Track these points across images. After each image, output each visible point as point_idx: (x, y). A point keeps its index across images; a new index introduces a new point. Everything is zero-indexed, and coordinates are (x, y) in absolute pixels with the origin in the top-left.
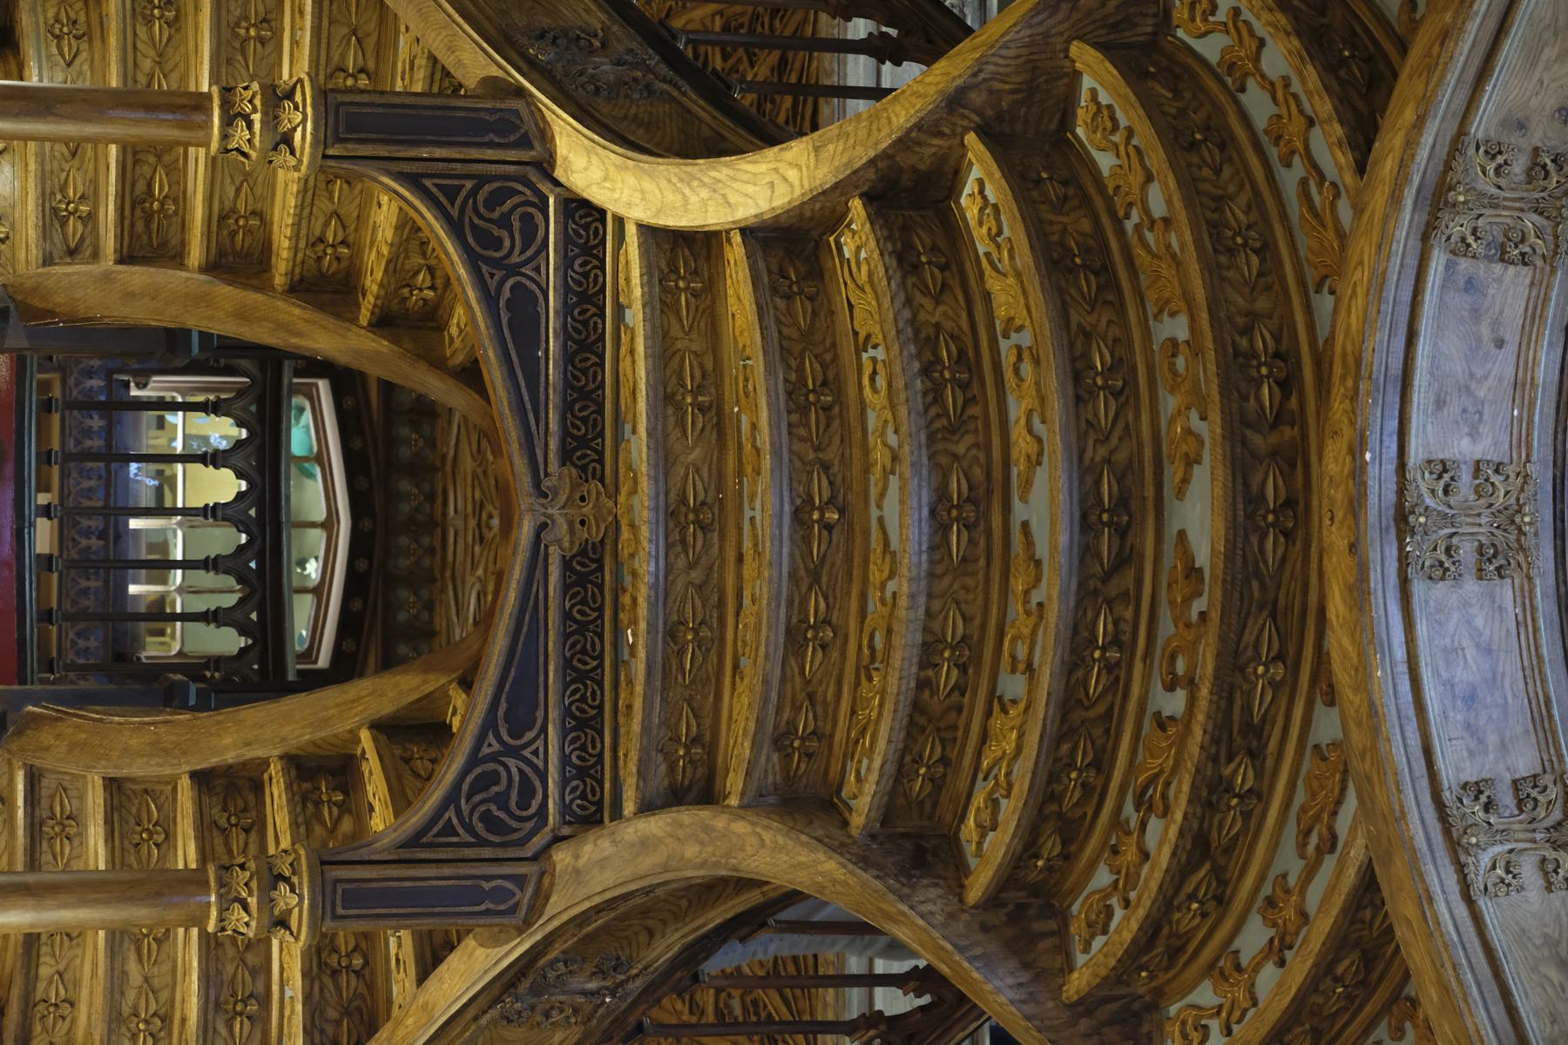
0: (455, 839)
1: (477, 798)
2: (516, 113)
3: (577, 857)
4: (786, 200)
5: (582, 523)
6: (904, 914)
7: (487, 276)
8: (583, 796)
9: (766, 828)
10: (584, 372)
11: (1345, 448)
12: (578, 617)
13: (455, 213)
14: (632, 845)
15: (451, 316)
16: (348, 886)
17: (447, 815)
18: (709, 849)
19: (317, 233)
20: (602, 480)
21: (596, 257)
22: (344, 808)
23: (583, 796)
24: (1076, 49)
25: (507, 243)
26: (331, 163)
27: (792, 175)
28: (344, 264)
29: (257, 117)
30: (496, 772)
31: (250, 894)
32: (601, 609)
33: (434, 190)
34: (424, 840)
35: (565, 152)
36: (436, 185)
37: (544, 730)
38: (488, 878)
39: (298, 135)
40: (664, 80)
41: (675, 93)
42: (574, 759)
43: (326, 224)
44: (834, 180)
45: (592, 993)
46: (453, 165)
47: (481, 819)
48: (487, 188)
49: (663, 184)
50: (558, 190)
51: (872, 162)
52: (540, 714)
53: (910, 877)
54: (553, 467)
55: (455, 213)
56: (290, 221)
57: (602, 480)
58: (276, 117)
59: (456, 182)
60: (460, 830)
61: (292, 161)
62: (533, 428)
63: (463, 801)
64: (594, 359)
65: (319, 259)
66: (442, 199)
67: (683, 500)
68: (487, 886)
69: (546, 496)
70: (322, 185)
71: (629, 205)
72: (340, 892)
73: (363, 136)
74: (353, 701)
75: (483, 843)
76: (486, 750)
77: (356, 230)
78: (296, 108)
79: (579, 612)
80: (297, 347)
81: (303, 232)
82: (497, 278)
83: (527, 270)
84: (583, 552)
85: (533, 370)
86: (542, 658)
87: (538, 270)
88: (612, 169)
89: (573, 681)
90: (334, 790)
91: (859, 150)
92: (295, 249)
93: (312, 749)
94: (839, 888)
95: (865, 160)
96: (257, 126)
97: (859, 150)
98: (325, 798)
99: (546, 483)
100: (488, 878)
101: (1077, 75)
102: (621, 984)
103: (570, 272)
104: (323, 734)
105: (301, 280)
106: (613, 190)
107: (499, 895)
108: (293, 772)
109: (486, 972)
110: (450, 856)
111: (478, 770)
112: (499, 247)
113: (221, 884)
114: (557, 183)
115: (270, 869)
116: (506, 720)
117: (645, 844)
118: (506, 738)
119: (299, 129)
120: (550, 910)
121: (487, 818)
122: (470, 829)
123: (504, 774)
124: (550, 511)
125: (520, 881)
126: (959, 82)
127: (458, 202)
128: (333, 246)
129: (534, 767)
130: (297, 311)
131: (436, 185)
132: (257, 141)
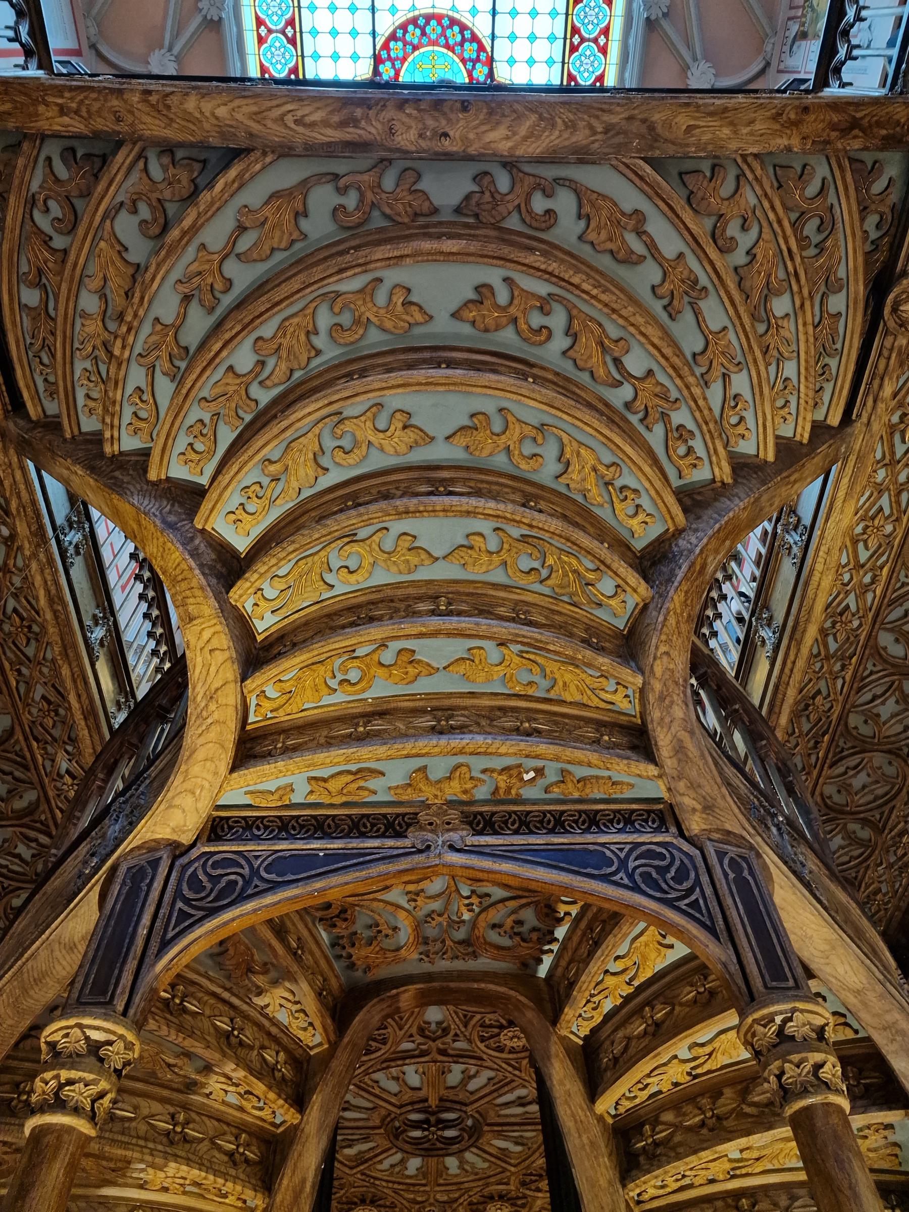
0: (701, 902)
2: (129, 869)
3: (694, 810)
4: (223, 636)
5: (448, 823)
6: (702, 551)
8: (646, 821)
9: (657, 648)
10: (337, 826)
11: (401, 116)
12: (516, 826)
13: (201, 914)
14: (679, 761)
15: (297, 1042)
16: (767, 977)
18: (675, 698)
19: (226, 1158)
20: (417, 814)
21: (254, 822)
22: (655, 1122)
23: (646, 821)
24: (152, 475)
25: (233, 877)
26: (131, 1012)
27: (206, 635)
28: (254, 1141)
29: (65, 1074)
30: (641, 875)
31: (804, 1060)
32: (510, 814)
33: (177, 930)
34: (708, 923)
35: (168, 830)
37: (603, 845)
39: (95, 1035)
40: (137, 790)
41: (148, 781)
42: (621, 826)
43: (220, 1148)
44: (213, 599)
45: (779, 829)
46: (161, 915)
47: (681, 883)
48: (186, 892)
49: (201, 741)
50: (198, 845)
51: (203, 574)
52: (591, 847)
53: (674, 556)
55: (201, 914)
56: (211, 1177)
57: (417, 814)
58: (70, 1056)
59: (175, 914)
60: (693, 898)
61: (119, 1046)
64: (329, 821)
65: (247, 1161)
67: (433, 728)
68: (732, 876)
69: (429, 847)
70: (187, 1146)
71: (216, 773)
72: (774, 983)
73: (113, 981)
74: (576, 1122)
75: (698, 882)
76: (626, 881)
77: (228, 1124)
78: (67, 1036)
79: (513, 824)
80: (313, 1186)
81: (223, 1169)
84: (470, 824)
85: (333, 857)
87: (257, 857)
88: (188, 785)
89: (564, 828)
90: (642, 1135)
91: (194, 583)
92: (235, 1179)
93: (614, 1158)
94: (689, 602)
95: (201, 577)
96: (74, 1074)
97: (194, 583)
98: (650, 1140)
99: (419, 847)
100: (726, 875)
101: (168, 479)
102: (769, 813)
104: (603, 1145)
105: (263, 1182)
106: (202, 787)
108: (634, 1173)
109: (794, 885)
110: (715, 904)
111: (643, 886)
112: (236, 882)
113: (805, 1092)
114: (193, 845)
115: (775, 1046)
116: (600, 869)
117: (679, 750)
118: (614, 868)
119: (89, 1032)
120: (738, 830)
122: (690, 892)
123: (641, 869)
124: (440, 843)
125: (721, 855)
126: (158, 522)
127: (192, 912)
128: (238, 1146)
129: (631, 851)
130: (285, 1182)
132: (90, 1077)
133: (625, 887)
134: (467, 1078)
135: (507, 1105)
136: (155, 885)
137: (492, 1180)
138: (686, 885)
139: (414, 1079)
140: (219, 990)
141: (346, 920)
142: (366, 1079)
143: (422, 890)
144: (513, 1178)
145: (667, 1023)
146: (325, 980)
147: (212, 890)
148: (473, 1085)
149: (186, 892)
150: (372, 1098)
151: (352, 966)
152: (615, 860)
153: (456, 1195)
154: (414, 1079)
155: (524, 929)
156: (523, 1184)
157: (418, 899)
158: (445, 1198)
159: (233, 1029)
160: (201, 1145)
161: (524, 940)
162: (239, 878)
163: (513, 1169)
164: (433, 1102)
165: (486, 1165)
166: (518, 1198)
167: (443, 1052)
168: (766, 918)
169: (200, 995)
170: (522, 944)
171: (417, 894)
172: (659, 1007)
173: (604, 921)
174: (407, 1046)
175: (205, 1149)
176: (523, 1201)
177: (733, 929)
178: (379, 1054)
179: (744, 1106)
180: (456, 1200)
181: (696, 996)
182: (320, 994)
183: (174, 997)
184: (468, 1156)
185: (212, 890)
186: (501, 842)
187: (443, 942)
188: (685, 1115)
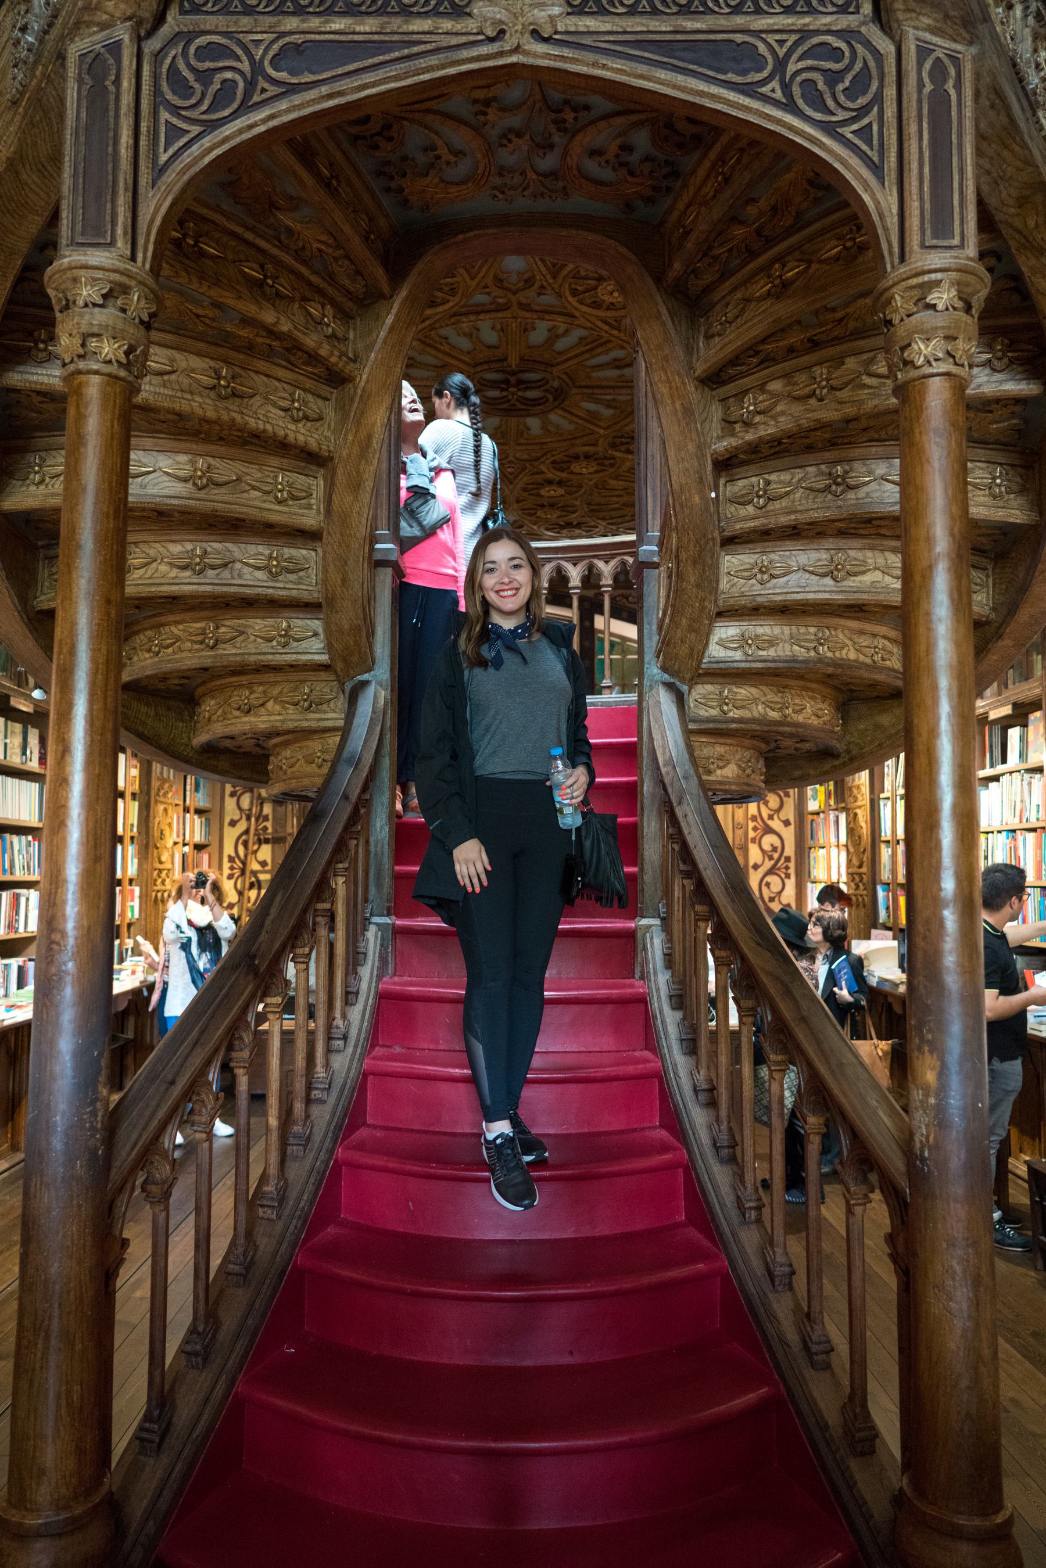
0: (875, 127)
1: (830, 103)
7: (265, 96)
13: (196, 129)
16: (928, 233)
17: (850, 136)
25: (229, 75)
33: (171, 152)
34: (876, 159)
36: (165, 151)
37: (757, 33)
38: (921, 85)
47: (852, 98)
48: (169, 96)
52: (739, 38)
54: (472, 25)
55: (196, 129)
59: (163, 129)
60: (865, 121)
62: (429, 47)
63: (834, 119)
66: (181, 143)
70: (238, 400)
74: (671, 388)
75: (879, 98)
76: (778, 95)
82: (266, 85)
83: (258, 54)
86: (679, 37)
99: (490, 32)
100: (921, 85)
103: (260, 8)
107: (939, 72)
110: (894, 132)
111: (800, 102)
116: (744, 73)
118: (765, 73)
121: (851, 93)
123: (805, 76)
125: (924, 52)
127: (184, 126)
128: (293, 401)
129: (796, 44)
131: (165, 151)
133: (776, 103)
134: (554, 336)
135: (599, 367)
136: (125, 84)
137: (578, 441)
138: (862, 101)
139: (490, 337)
140: (239, 230)
141: (390, 139)
142: (433, 333)
143: (495, 99)
144: (601, 440)
145: (798, 283)
146: (371, 220)
147: (203, 95)
148: (560, 345)
149: (169, 96)
150: (440, 355)
151: (405, 203)
152: (770, 60)
153: (539, 455)
154: (490, 337)
155: (634, 158)
156: (613, 446)
157: (490, 111)
158: (526, 457)
159: (266, 277)
160: (252, 401)
161: (631, 173)
162: (238, 77)
163: (602, 432)
164: (513, 361)
165: (572, 427)
166: (605, 458)
167: (526, 307)
168: (955, 152)
169: (217, 235)
170: (630, 179)
171: (487, 103)
172: (790, 265)
173: (742, 150)
174: (480, 298)
175: (258, 404)
176: (612, 461)
177: (906, 168)
178: (447, 306)
179: (864, 377)
180: (538, 459)
181: (840, 252)
182: (367, 238)
183: (185, 236)
184: (552, 417)
185: (203, 95)
186: (608, 27)
187: (523, 173)
188: (796, 384)
